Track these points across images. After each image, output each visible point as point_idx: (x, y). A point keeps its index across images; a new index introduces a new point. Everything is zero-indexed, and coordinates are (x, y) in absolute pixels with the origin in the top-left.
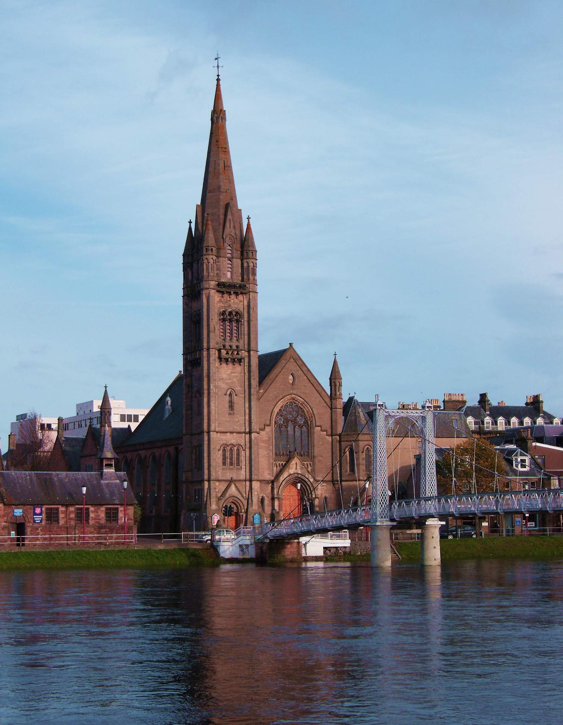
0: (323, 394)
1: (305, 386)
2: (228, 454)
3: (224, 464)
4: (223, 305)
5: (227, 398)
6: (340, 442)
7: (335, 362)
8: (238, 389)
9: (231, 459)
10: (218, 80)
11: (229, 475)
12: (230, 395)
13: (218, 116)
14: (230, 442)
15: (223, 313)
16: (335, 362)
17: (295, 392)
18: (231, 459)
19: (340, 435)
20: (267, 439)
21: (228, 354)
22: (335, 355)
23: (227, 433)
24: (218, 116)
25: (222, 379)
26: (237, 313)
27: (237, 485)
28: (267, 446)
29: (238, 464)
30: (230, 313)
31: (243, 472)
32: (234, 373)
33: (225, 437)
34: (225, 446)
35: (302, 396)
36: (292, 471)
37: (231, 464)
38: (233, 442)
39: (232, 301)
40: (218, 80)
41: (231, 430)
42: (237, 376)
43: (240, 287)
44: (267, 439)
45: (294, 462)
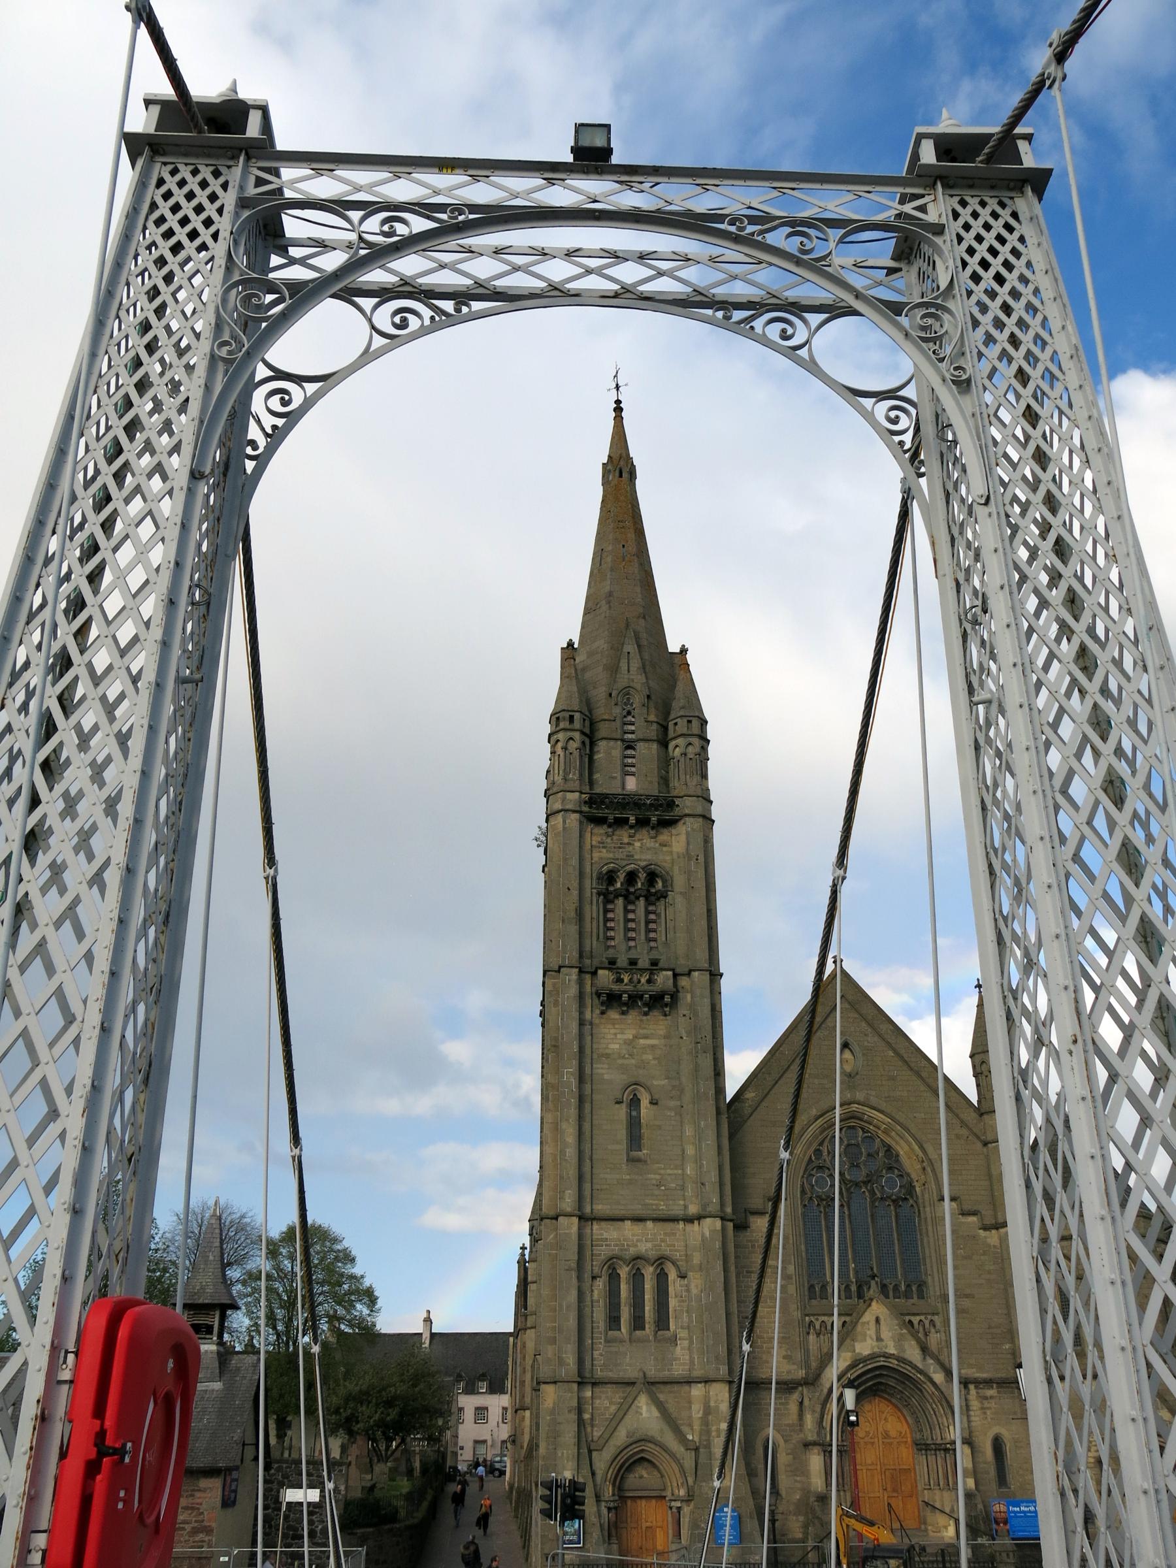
1: (893, 1078)
3: (614, 1321)
4: (611, 855)
5: (622, 1112)
8: (659, 1082)
10: (618, 409)
12: (635, 1102)
13: (620, 471)
14: (632, 1251)
15: (610, 877)
17: (860, 1096)
21: (622, 981)
23: (622, 1220)
24: (620, 471)
25: (607, 1056)
26: (652, 877)
27: (662, 1397)
29: (662, 1322)
30: (631, 877)
32: (646, 1037)
33: (615, 1235)
34: (611, 1264)
35: (883, 1105)
36: (864, 1348)
37: (638, 1322)
38: (644, 1248)
39: (638, 844)
40: (618, 409)
41: (638, 1210)
42: (653, 1046)
43: (655, 806)
45: (869, 1317)
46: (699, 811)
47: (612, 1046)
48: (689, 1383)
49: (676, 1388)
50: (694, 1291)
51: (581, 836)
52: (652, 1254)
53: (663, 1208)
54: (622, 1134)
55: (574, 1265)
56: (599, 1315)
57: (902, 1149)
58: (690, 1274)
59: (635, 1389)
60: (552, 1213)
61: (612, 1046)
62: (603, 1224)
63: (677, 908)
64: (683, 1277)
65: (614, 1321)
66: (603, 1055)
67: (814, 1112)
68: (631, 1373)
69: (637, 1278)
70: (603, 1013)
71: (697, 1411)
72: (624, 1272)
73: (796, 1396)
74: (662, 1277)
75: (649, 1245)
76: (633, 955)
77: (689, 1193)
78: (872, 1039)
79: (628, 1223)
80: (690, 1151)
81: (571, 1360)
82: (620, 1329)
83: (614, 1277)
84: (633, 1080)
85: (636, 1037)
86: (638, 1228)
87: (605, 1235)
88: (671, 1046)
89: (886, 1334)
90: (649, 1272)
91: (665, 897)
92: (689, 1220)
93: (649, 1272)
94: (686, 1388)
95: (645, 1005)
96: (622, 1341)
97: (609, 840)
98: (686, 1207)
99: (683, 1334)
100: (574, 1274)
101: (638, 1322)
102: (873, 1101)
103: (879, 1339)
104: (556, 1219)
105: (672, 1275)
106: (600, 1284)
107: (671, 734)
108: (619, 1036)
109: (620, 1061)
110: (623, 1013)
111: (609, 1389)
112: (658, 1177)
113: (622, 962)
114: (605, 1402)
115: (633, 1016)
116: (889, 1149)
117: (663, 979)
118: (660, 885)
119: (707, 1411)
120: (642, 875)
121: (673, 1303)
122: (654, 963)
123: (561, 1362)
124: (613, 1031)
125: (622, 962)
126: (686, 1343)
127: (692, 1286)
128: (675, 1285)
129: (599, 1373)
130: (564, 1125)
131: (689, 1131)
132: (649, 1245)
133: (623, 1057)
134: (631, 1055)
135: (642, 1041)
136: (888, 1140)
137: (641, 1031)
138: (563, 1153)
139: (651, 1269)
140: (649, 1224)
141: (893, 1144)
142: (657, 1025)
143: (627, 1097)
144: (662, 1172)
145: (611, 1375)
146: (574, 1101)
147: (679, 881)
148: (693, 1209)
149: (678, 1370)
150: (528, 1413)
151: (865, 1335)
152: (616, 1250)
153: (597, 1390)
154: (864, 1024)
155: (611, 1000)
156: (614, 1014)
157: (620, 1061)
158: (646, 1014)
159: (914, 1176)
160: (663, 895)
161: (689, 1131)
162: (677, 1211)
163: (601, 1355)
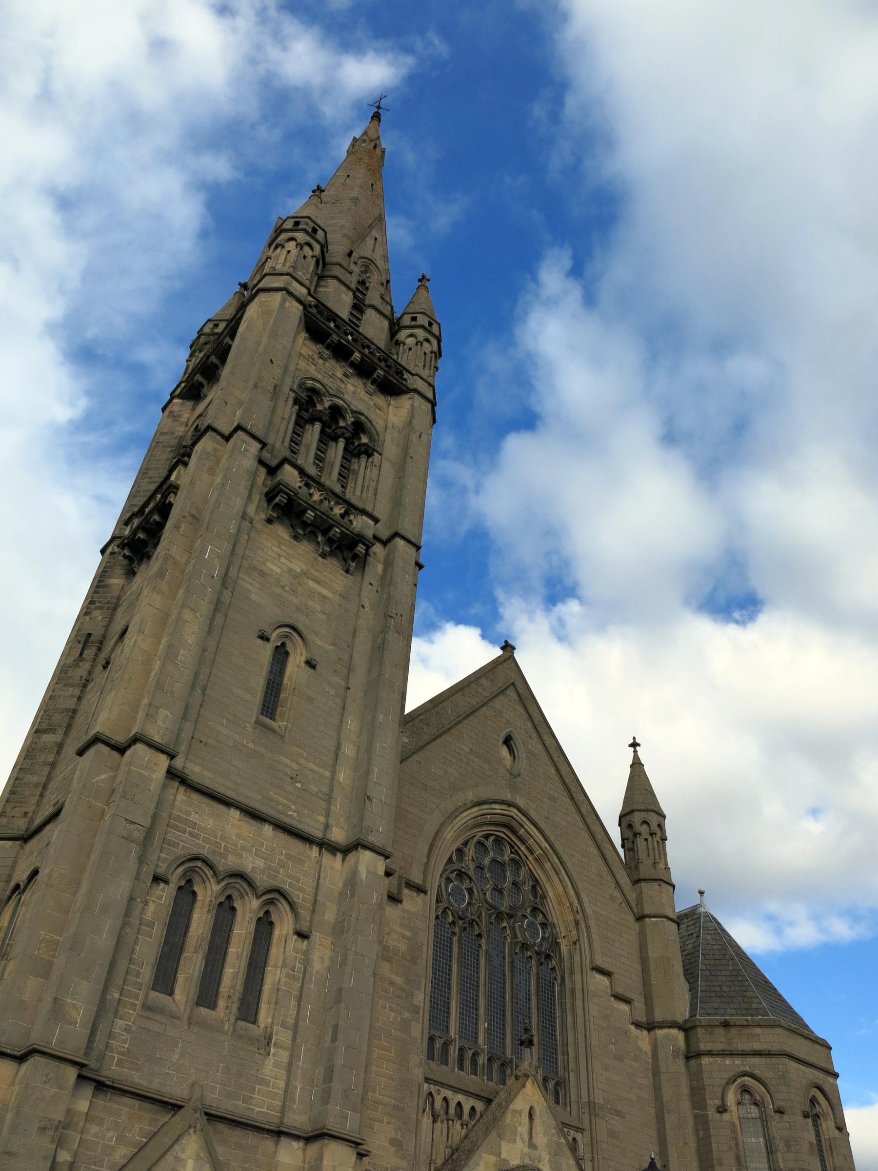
0: (609, 853)
2: (200, 922)
5: (266, 652)
6: (691, 1055)
7: (637, 765)
8: (322, 645)
12: (281, 654)
14: (231, 862)
16: (637, 765)
19: (687, 1028)
20: (403, 947)
22: (634, 745)
25: (262, 574)
26: (359, 427)
27: (221, 1151)
28: (399, 980)
31: (272, 1068)
33: (209, 822)
34: (197, 864)
37: (207, 994)
38: (250, 863)
41: (255, 802)
44: (403, 947)
45: (520, 1104)
47: (269, 565)
48: (278, 1134)
49: (251, 1138)
50: (318, 965)
51: (295, 337)
53: (291, 816)
55: (139, 835)
56: (147, 950)
57: (553, 889)
58: (316, 936)
59: (179, 1120)
60: (120, 738)
61: (269, 565)
62: (196, 797)
64: (302, 935)
65: (164, 979)
66: (255, 569)
67: (471, 796)
68: (175, 1090)
69: (226, 910)
70: (269, 521)
72: (208, 892)
74: (265, 925)
75: (260, 863)
77: (338, 806)
79: (235, 814)
80: (348, 750)
82: (171, 993)
83: (186, 893)
84: (287, 621)
85: (304, 573)
86: (248, 828)
87: (194, 817)
88: (346, 610)
89: (540, 1139)
90: (248, 909)
91: (369, 456)
93: (248, 909)
94: (268, 1143)
95: (330, 541)
96: (173, 1016)
97: (321, 361)
98: (327, 826)
99: (282, 1036)
100: (135, 850)
101: (207, 994)
103: (532, 1146)
104: (121, 750)
105: (284, 926)
108: (283, 560)
109: (278, 590)
110: (296, 537)
111: (125, 1107)
112: (295, 766)
115: (305, 548)
116: (536, 884)
121: (273, 976)
123: (57, 1010)
124: (276, 549)
126: (284, 1055)
127: (316, 955)
128: (283, 942)
130: (187, 615)
132: (260, 863)
133: (283, 587)
134: (294, 591)
135: (311, 583)
136: (539, 873)
137: (313, 571)
138: (171, 652)
139: (255, 903)
140: (268, 829)
141: (542, 878)
142: (330, 580)
143: (275, 637)
144: (302, 761)
145: (137, 1079)
149: (262, 1107)
151: (515, 1132)
152: (205, 850)
153: (102, 1102)
154: (529, 724)
156: (282, 531)
157: (278, 590)
158: (323, 555)
159: (561, 930)
162: (314, 827)
163: (128, 1030)
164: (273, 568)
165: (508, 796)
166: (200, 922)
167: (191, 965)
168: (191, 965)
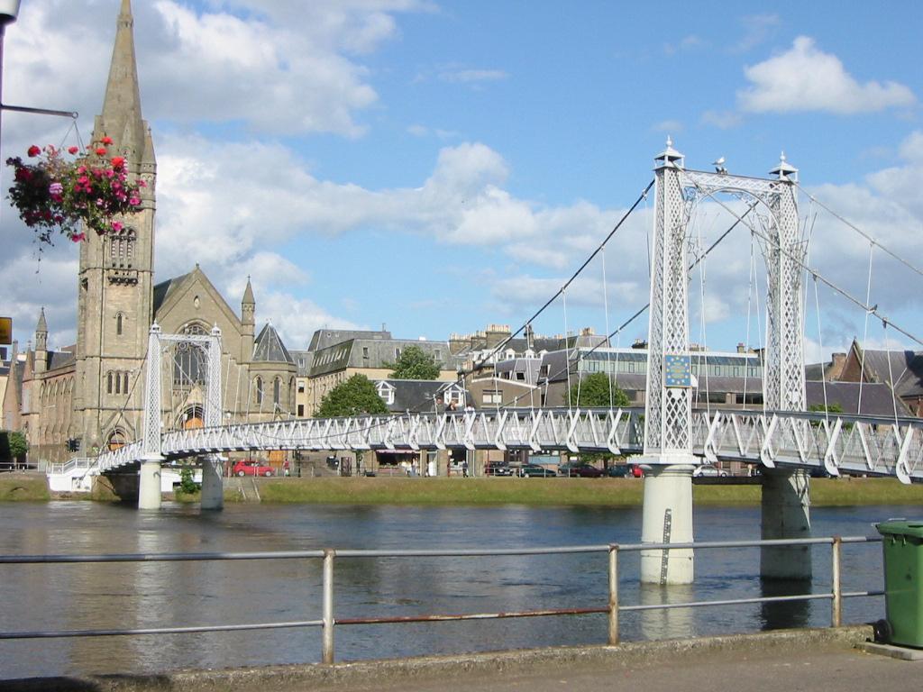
2: (114, 381)
3: (110, 391)
5: (116, 321)
9: (118, 386)
11: (115, 404)
12: (120, 318)
14: (117, 368)
18: (118, 386)
29: (126, 391)
35: (207, 320)
37: (118, 391)
46: (151, 206)
52: (124, 370)
54: (116, 329)
56: (105, 388)
63: (140, 245)
65: (110, 391)
68: (115, 407)
69: (118, 378)
71: (135, 419)
72: (114, 375)
73: (167, 415)
74: (126, 378)
76: (122, 263)
78: (206, 296)
80: (139, 336)
81: (96, 402)
83: (110, 377)
92: (136, 359)
102: (204, 318)
106: (106, 379)
107: (141, 171)
113: (118, 266)
114: (105, 415)
117: (133, 275)
118: (133, 234)
119: (139, 419)
120: (127, 231)
122: (129, 266)
125: (118, 266)
129: (105, 407)
131: (139, 329)
142: (130, 289)
145: (108, 407)
146: (99, 318)
147: (141, 235)
148: (138, 356)
150: (36, 416)
155: (114, 281)
156: (114, 286)
160: (134, 239)
161: (139, 329)
164: (113, 298)
165: (195, 317)
166: (114, 381)
167: (114, 388)
168: (114, 388)
